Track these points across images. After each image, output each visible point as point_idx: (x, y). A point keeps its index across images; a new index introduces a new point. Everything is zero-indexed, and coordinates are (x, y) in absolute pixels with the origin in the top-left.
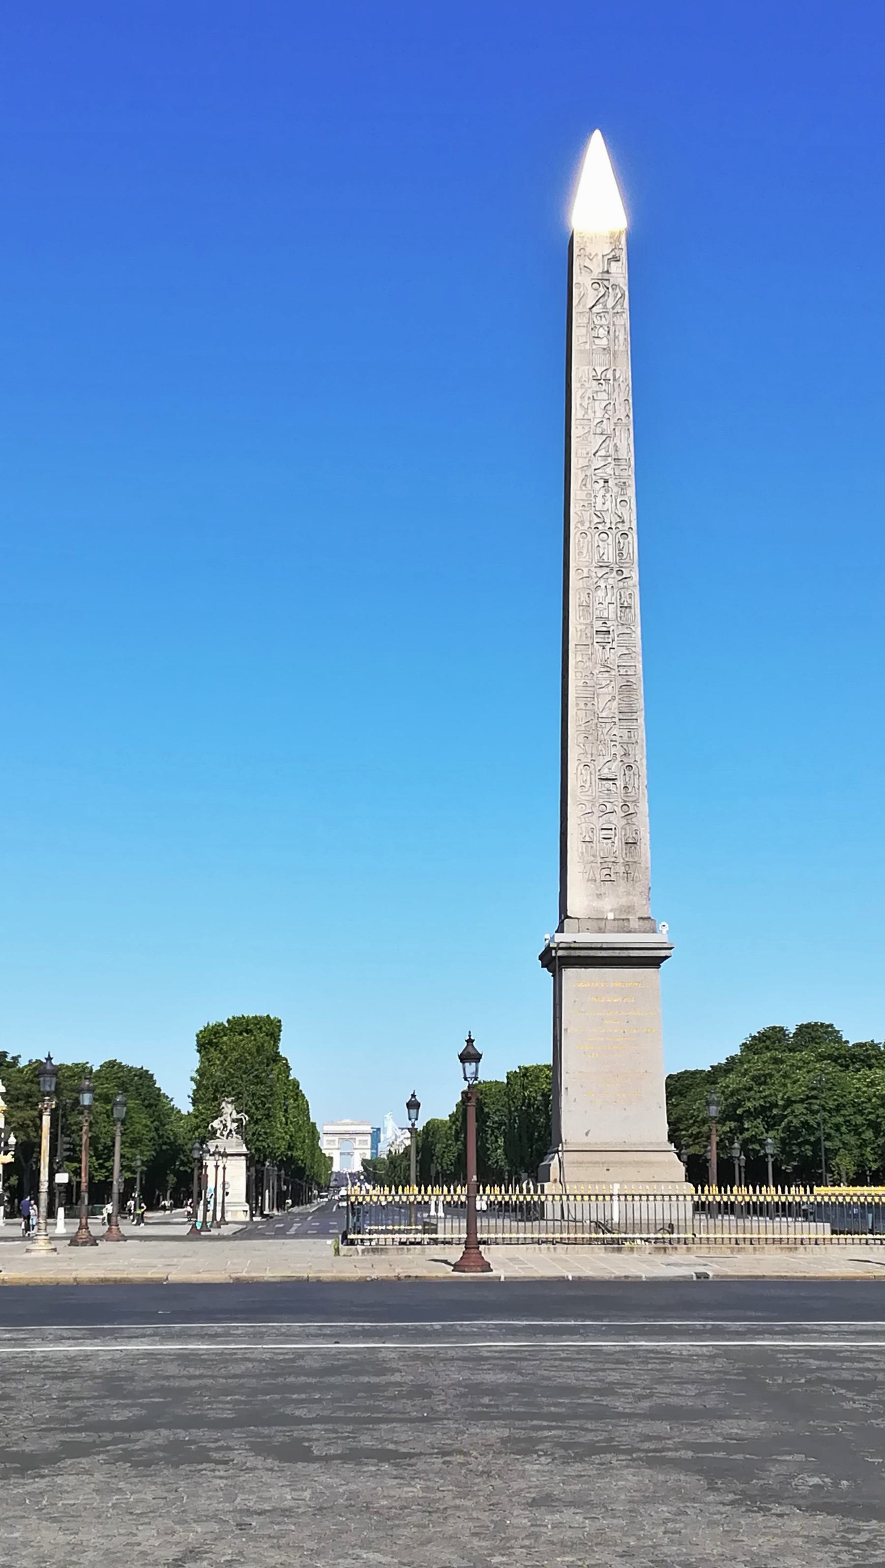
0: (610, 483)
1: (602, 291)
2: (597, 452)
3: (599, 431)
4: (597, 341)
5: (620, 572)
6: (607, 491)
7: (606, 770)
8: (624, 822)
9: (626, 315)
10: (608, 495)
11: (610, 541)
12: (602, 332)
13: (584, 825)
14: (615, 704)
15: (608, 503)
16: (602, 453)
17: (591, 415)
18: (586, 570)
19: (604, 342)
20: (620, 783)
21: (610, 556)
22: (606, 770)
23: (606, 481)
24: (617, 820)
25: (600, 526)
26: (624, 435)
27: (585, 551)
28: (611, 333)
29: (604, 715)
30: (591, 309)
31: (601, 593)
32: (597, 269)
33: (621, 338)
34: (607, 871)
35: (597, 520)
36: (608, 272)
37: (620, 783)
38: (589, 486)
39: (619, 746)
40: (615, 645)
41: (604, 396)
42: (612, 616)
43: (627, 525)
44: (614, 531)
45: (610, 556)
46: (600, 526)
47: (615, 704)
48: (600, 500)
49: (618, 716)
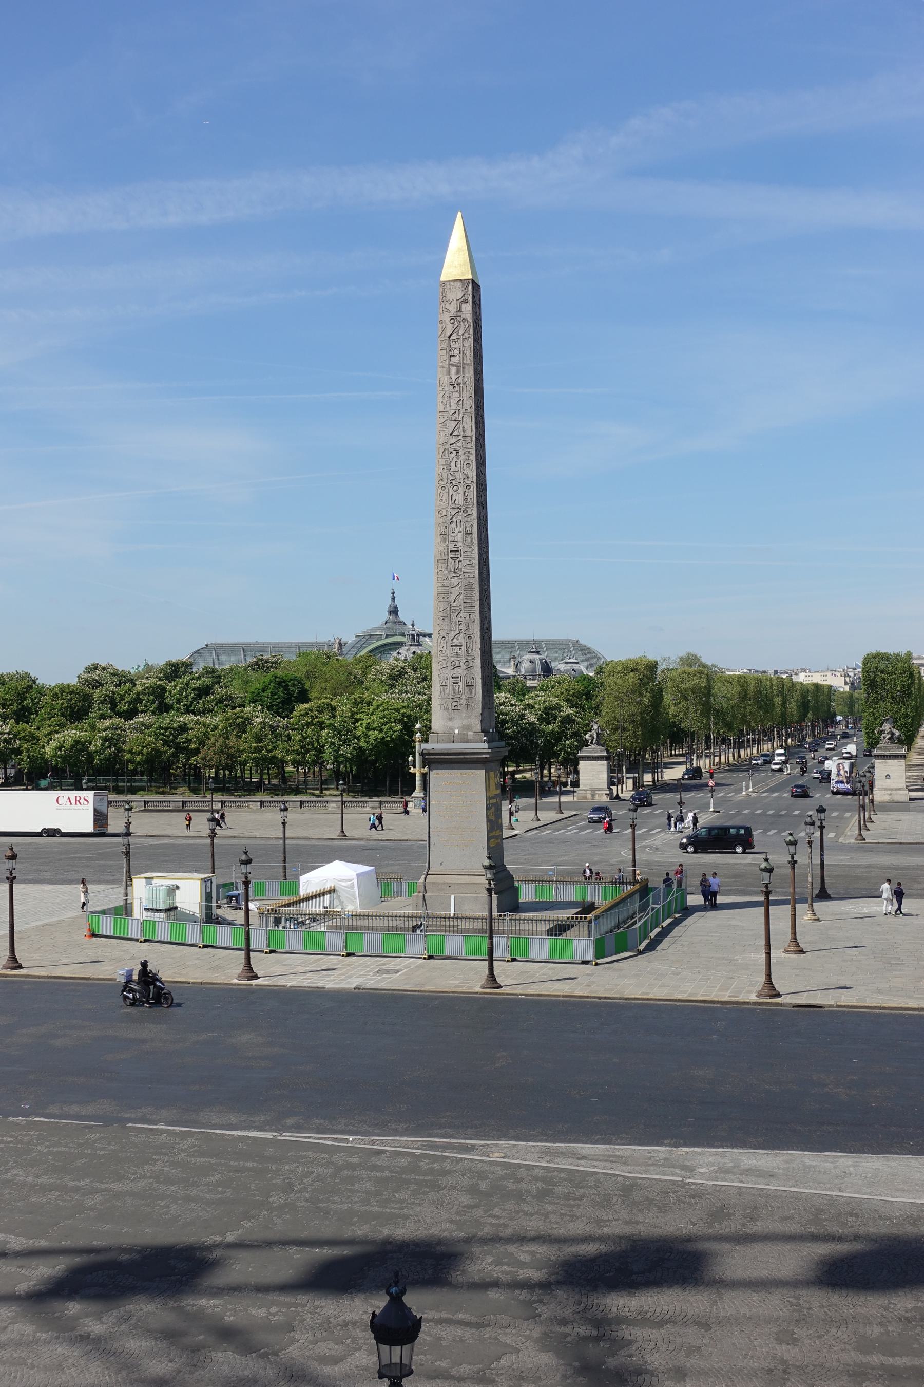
3: (453, 418)
4: (453, 359)
8: (466, 672)
9: (471, 339)
11: (459, 491)
12: (456, 352)
14: (461, 597)
15: (458, 466)
19: (456, 359)
20: (464, 648)
24: (461, 672)
25: (454, 482)
26: (469, 420)
27: (444, 498)
31: (453, 525)
32: (453, 308)
33: (468, 355)
34: (454, 704)
36: (460, 311)
37: (464, 648)
40: (462, 559)
41: (457, 395)
42: (460, 540)
43: (470, 479)
46: (454, 482)
49: (463, 605)
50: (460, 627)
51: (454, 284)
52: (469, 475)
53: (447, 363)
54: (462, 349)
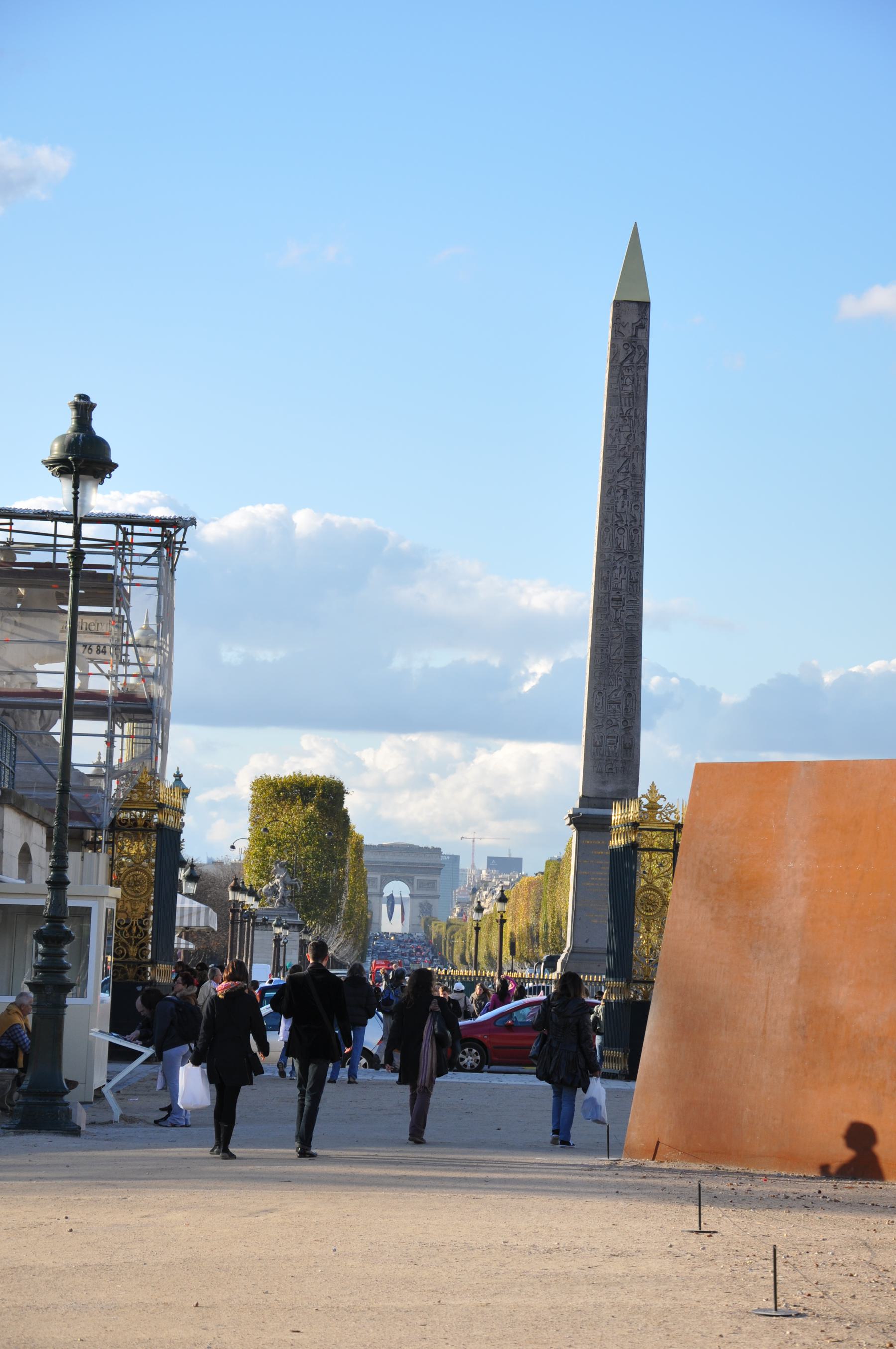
0: (628, 493)
1: (630, 350)
2: (621, 468)
3: (622, 453)
4: (625, 388)
5: (631, 557)
6: (626, 498)
7: (613, 696)
10: (626, 501)
12: (628, 381)
13: (596, 734)
15: (626, 507)
16: (624, 470)
17: (617, 442)
18: (607, 555)
21: (625, 546)
22: (613, 696)
23: (625, 491)
24: (619, 732)
25: (619, 524)
28: (635, 382)
29: (614, 657)
30: (622, 364)
31: (617, 572)
34: (609, 766)
35: (617, 519)
36: (635, 336)
37: (623, 706)
38: (613, 494)
39: (623, 680)
41: (627, 428)
44: (629, 528)
45: (625, 546)
46: (619, 524)
47: (622, 650)
48: (619, 505)
50: (619, 683)
51: (631, 305)
52: (638, 517)
53: (618, 392)
54: (636, 378)
